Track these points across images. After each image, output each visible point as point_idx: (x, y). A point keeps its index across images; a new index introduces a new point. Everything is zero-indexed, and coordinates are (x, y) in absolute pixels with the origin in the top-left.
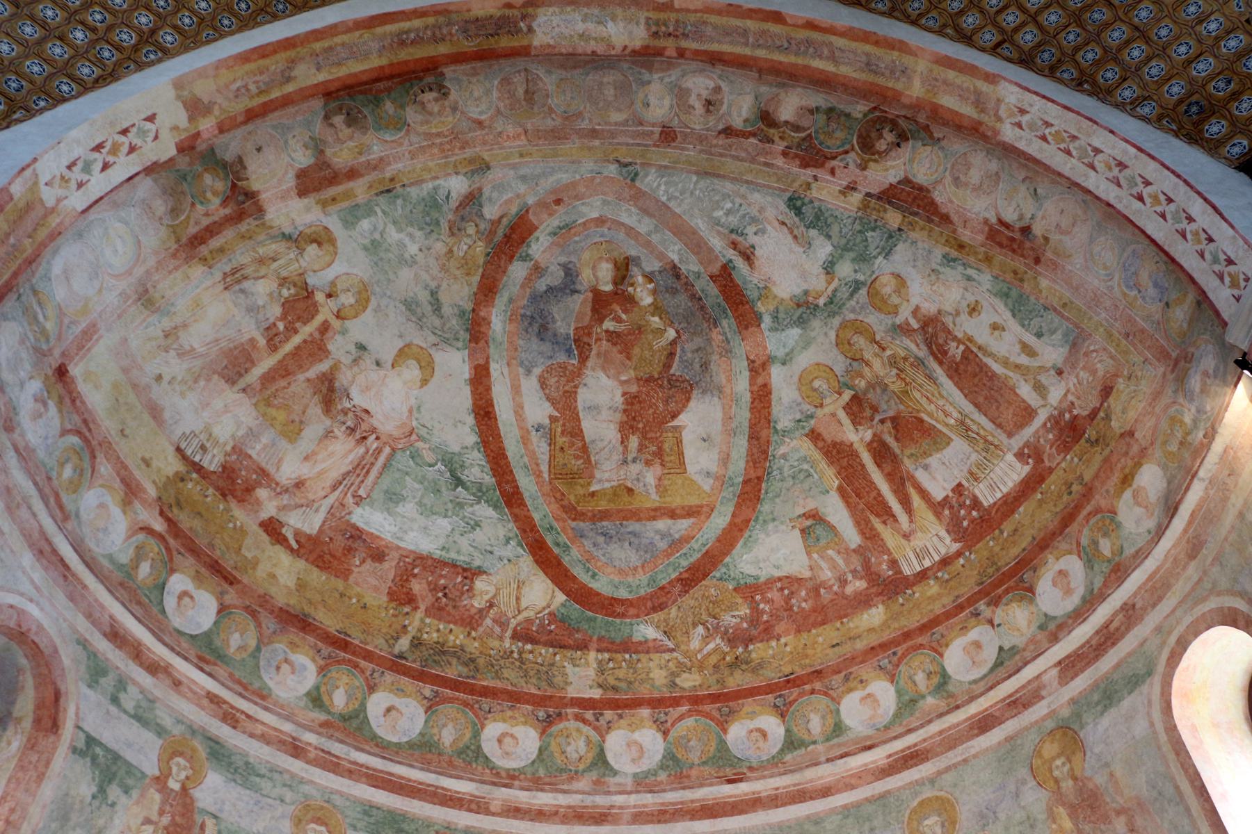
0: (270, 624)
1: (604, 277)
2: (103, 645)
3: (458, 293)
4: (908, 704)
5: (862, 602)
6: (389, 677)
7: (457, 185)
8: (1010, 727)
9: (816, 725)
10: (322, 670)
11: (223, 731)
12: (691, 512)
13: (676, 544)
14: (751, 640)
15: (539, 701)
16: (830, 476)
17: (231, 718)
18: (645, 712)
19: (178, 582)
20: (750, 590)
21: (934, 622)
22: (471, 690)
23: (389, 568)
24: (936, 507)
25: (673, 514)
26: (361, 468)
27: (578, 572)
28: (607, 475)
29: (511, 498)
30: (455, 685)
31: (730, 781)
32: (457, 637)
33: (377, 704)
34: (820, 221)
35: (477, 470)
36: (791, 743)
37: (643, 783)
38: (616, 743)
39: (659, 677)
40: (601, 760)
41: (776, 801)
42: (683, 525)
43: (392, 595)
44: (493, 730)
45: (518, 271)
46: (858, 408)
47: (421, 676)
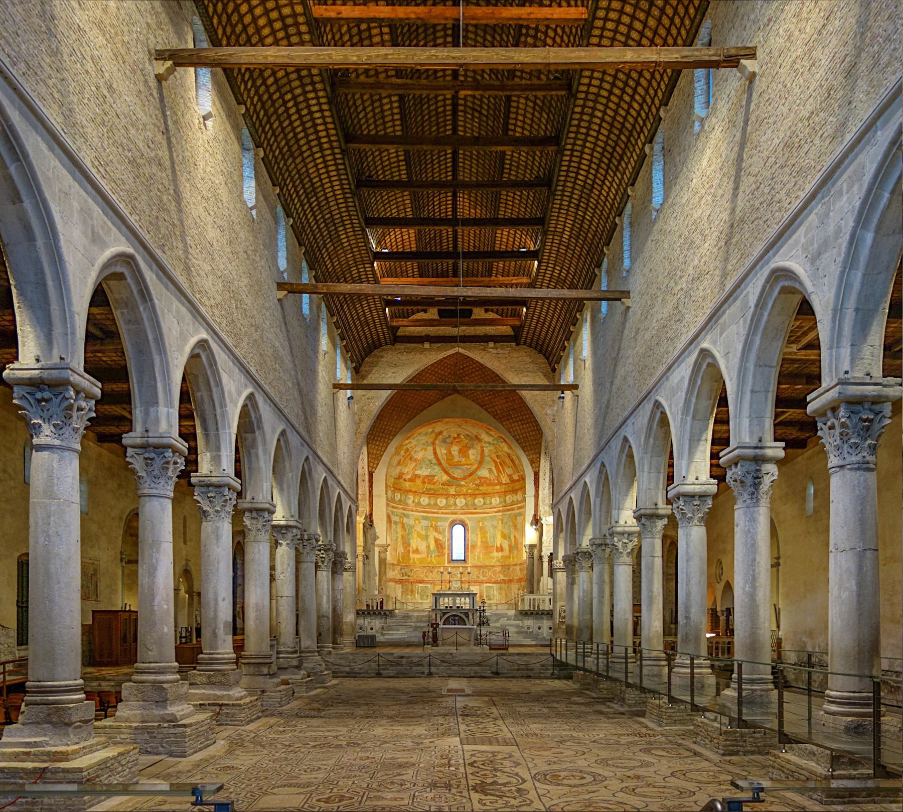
3: (431, 440)
5: (496, 485)
9: (488, 502)
13: (468, 469)
20: (480, 478)
28: (456, 459)
29: (440, 464)
32: (432, 487)
34: (491, 435)
35: (434, 461)
36: (484, 504)
37: (462, 508)
38: (457, 501)
40: (455, 504)
44: (439, 500)
45: (440, 437)
46: (497, 456)
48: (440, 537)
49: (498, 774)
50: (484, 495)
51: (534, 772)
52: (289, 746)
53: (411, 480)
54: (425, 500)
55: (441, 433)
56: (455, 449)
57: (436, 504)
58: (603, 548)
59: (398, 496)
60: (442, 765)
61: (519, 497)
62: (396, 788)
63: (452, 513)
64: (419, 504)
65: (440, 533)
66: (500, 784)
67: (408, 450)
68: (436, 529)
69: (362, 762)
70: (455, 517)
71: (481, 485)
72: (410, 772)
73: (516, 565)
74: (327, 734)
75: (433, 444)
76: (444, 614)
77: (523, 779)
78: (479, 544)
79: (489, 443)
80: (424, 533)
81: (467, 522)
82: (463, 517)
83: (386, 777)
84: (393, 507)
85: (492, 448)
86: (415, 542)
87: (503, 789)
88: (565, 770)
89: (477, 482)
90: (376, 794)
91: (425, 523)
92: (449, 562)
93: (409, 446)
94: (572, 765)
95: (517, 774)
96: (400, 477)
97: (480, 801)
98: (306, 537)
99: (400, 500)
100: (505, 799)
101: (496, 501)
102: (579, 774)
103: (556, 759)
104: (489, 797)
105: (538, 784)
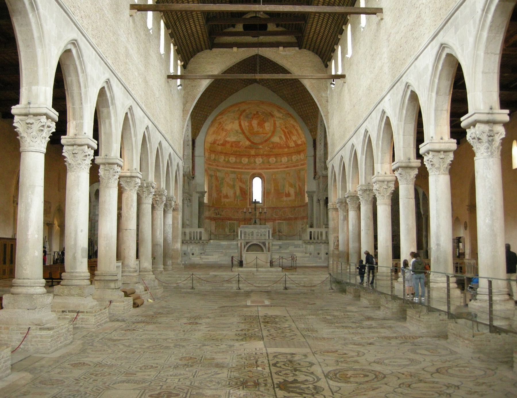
0: (219, 154)
1: (255, 113)
2: (209, 166)
4: (288, 161)
5: (285, 148)
6: (231, 156)
7: (237, 109)
8: (296, 168)
9: (279, 160)
10: (225, 157)
11: (218, 168)
12: (266, 133)
14: (272, 149)
15: (248, 155)
16: (282, 132)
17: (218, 166)
18: (260, 156)
19: (211, 155)
20: (273, 143)
21: (292, 153)
22: (240, 155)
23: (230, 144)
24: (294, 141)
25: (263, 134)
26: (226, 134)
27: (252, 140)
28: (256, 129)
29: (244, 133)
30: (238, 155)
31: (270, 166)
32: (238, 149)
33: (230, 159)
35: (240, 131)
36: (276, 162)
38: (257, 160)
39: (262, 152)
40: (255, 162)
41: (274, 169)
42: (265, 135)
43: (231, 147)
44: (243, 159)
45: (244, 113)
46: (286, 127)
47: (235, 155)
48: (243, 186)
49: (297, 373)
50: (277, 155)
52: (129, 346)
53: (223, 145)
54: (232, 159)
55: (244, 111)
56: (255, 123)
57: (241, 162)
58: (368, 193)
59: (213, 156)
60: (251, 365)
61: (302, 156)
63: (253, 169)
64: (228, 162)
65: (244, 183)
67: (220, 123)
68: (241, 180)
69: (186, 362)
70: (255, 171)
71: (273, 148)
73: (300, 206)
75: (239, 118)
76: (247, 243)
77: (317, 377)
78: (273, 191)
79: (279, 118)
80: (232, 183)
81: (264, 175)
82: (260, 171)
83: (206, 376)
84: (209, 164)
85: (281, 121)
86: (225, 190)
87: (303, 386)
89: (271, 146)
90: (197, 391)
91: (233, 176)
92: (250, 205)
93: (221, 120)
96: (214, 143)
98: (145, 185)
99: (215, 159)
100: (304, 395)
101: (284, 159)
102: (363, 373)
103: (342, 360)
105: (331, 382)
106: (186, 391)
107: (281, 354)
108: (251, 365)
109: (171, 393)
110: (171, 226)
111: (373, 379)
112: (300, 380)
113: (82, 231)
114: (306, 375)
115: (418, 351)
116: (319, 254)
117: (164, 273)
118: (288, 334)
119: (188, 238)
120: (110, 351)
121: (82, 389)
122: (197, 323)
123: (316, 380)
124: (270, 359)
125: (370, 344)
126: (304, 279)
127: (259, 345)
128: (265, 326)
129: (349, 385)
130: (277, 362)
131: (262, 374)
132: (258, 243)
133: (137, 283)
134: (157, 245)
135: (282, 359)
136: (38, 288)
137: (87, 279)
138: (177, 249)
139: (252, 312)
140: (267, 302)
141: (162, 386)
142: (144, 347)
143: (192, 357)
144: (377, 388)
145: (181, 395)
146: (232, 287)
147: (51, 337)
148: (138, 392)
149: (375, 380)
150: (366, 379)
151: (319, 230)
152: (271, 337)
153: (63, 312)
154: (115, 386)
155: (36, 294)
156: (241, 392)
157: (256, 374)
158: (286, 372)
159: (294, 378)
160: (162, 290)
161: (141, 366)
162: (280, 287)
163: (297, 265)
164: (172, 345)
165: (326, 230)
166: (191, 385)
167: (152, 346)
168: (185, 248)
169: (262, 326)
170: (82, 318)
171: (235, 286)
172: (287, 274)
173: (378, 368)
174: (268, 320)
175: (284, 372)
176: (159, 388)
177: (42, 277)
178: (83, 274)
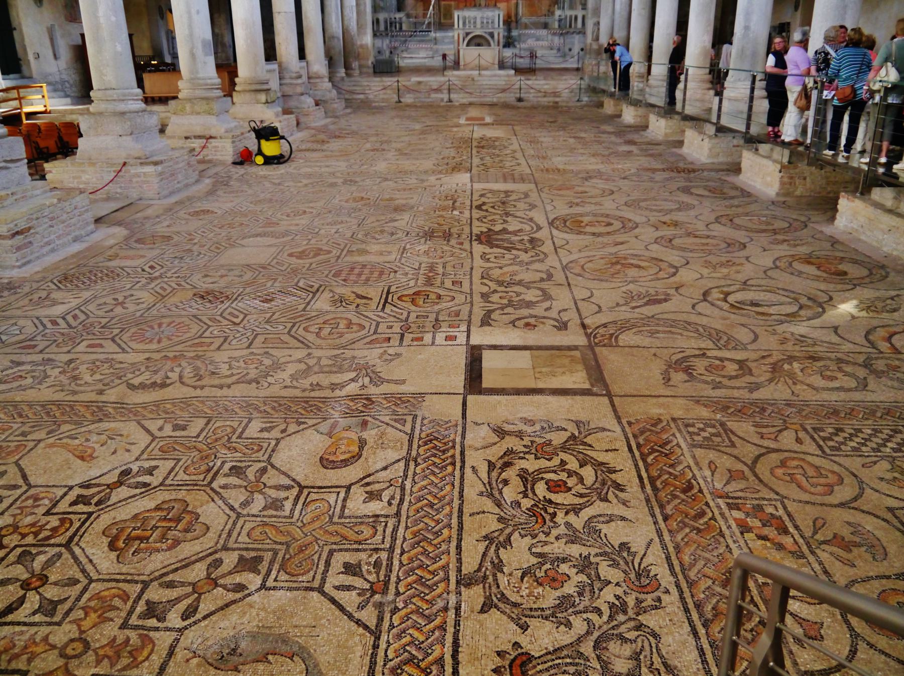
49: (509, 219)
51: (551, 217)
52: (279, 184)
60: (444, 209)
62: (385, 238)
66: (510, 233)
69: (354, 205)
72: (406, 216)
74: (323, 170)
76: (467, 34)
83: (377, 223)
88: (587, 214)
94: (598, 207)
95: (531, 220)
97: (483, 256)
100: (514, 252)
103: (578, 200)
104: (495, 250)
105: (555, 232)
106: (342, 247)
107: (491, 191)
108: (444, 209)
109: (321, 249)
110: (354, 9)
111: (618, 230)
112: (511, 229)
113: (198, 12)
114: (521, 222)
115: (693, 190)
116: (570, 50)
117: (346, 78)
118: (508, 164)
119: (382, 27)
120: (250, 192)
121: (195, 248)
122: (384, 150)
123: (535, 229)
124: (474, 199)
125: (624, 178)
126: (546, 87)
127: (463, 179)
128: (478, 152)
129: (582, 237)
130: (484, 204)
131: (458, 221)
132: (484, 34)
133: (302, 94)
134: (333, 37)
135: (490, 199)
136: (132, 102)
137: (217, 89)
138: (367, 45)
139: (465, 132)
140: (488, 120)
141: (310, 240)
142: (300, 184)
143: (365, 197)
144: (622, 243)
145: (335, 252)
146: (442, 100)
147: (160, 174)
148: (273, 249)
149: (622, 231)
150: (609, 229)
151: (573, 13)
152: (483, 168)
153: (186, 138)
154: (243, 242)
155: (130, 112)
156: (421, 247)
157: (449, 221)
158: (494, 217)
159: (505, 226)
160: (343, 104)
161: (289, 211)
162: (510, 98)
163: (537, 66)
164: (340, 181)
165: (584, 12)
166: (352, 237)
167: (312, 184)
168: (379, 43)
169: (474, 152)
170: (216, 147)
171: (445, 97)
172: (523, 78)
173: (628, 214)
174: (484, 144)
175: (490, 218)
176: (305, 243)
177: (136, 85)
178: (209, 81)
